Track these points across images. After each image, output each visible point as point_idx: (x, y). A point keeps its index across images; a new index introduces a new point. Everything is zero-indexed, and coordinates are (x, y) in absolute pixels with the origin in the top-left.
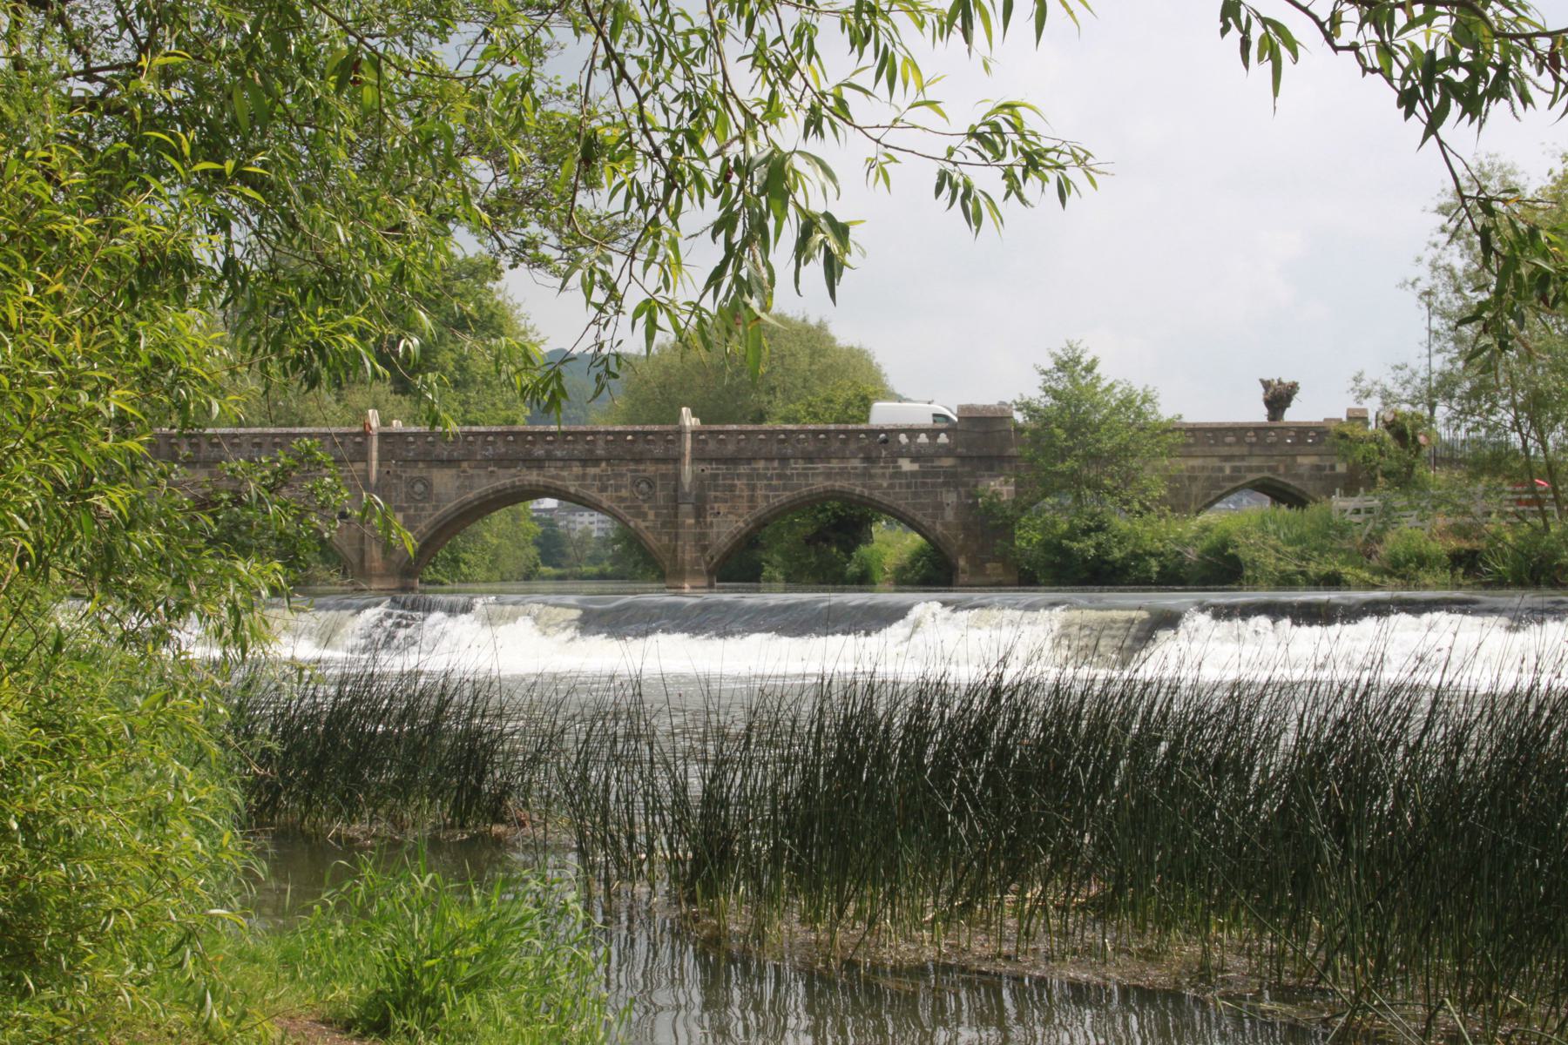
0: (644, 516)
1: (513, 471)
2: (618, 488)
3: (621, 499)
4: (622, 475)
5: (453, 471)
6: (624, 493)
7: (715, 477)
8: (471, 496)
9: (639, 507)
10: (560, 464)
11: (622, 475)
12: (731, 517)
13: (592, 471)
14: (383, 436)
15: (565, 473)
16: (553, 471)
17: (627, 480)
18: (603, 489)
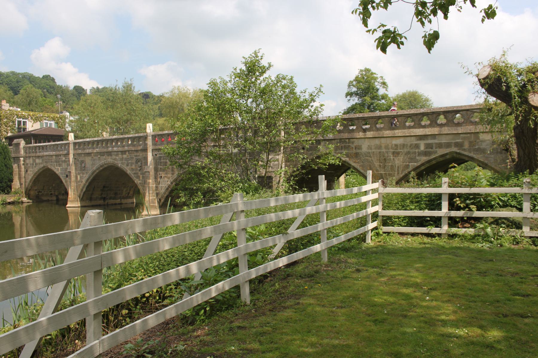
0: (138, 177)
1: (104, 157)
2: (132, 164)
3: (133, 170)
4: (132, 158)
5: (90, 158)
6: (133, 167)
7: (160, 157)
8: (95, 168)
9: (137, 173)
10: (116, 153)
11: (132, 158)
12: (166, 179)
13: (125, 156)
14: (75, 144)
15: (117, 158)
16: (114, 157)
17: (134, 161)
18: (127, 165)
